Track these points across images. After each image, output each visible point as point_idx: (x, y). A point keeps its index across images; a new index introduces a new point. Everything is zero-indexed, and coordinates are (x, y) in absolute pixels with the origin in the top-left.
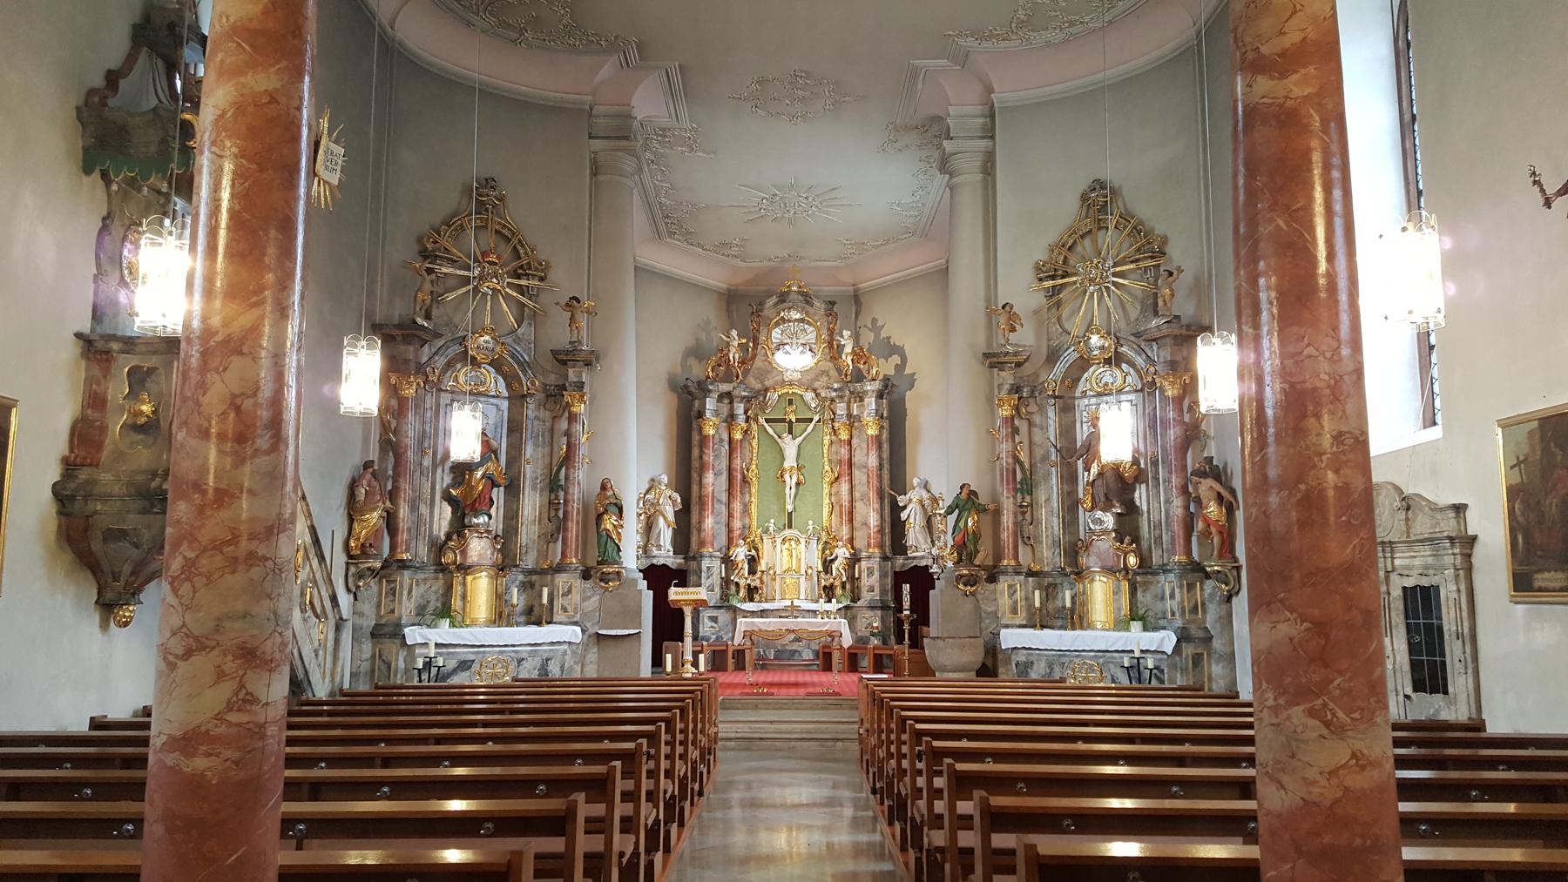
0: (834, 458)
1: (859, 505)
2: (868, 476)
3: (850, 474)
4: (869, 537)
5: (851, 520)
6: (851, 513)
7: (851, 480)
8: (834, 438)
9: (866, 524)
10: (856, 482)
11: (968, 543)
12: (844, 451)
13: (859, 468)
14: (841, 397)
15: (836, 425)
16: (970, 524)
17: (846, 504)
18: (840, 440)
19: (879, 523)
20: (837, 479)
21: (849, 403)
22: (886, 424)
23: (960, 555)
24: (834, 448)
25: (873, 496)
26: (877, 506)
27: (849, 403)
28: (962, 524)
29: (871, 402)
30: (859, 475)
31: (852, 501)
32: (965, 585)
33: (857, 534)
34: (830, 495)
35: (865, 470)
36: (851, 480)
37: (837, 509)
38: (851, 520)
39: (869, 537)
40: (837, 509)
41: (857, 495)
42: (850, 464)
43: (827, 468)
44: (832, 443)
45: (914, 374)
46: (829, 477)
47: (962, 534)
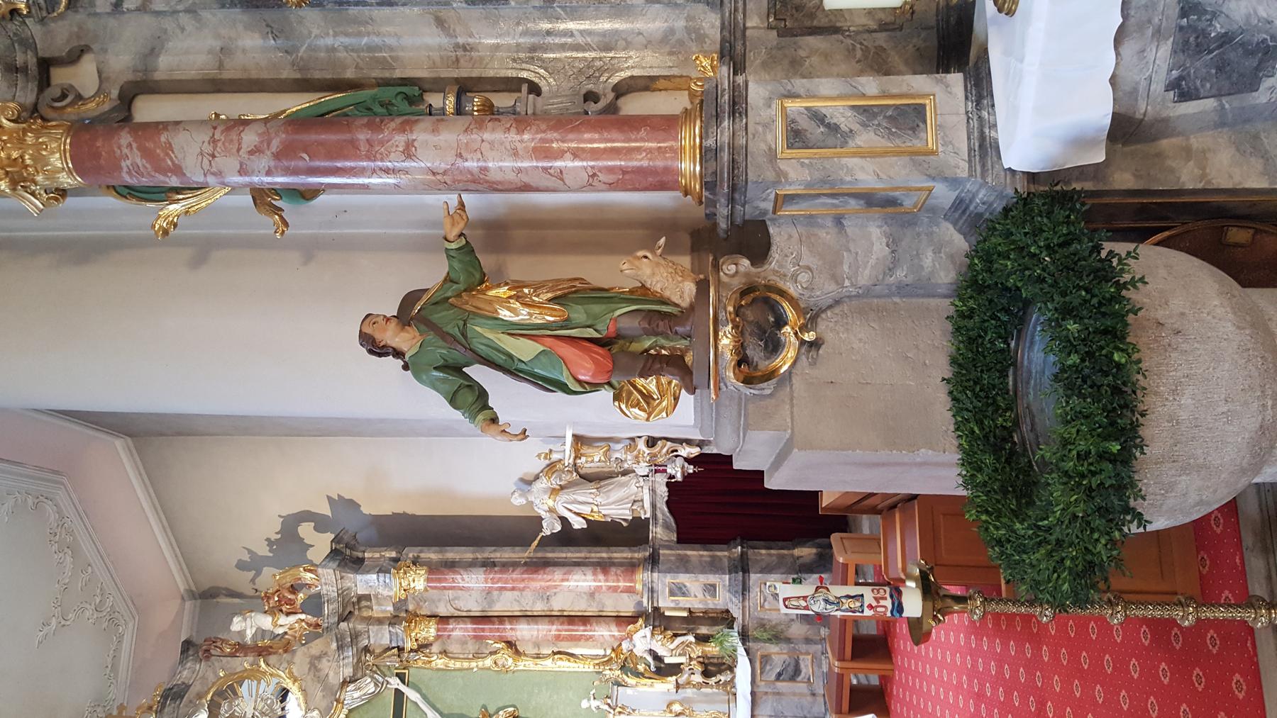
0: (472, 647)
1: (560, 604)
2: (501, 589)
3: (501, 619)
4: (615, 589)
5: (584, 620)
6: (571, 619)
7: (513, 618)
8: (435, 649)
9: (592, 595)
10: (515, 609)
11: (603, 329)
12: (459, 631)
13: (491, 603)
14: (355, 636)
15: (409, 645)
16: (523, 315)
17: (554, 629)
18: (438, 637)
19: (589, 571)
20: (510, 644)
21: (369, 620)
22: (411, 553)
23: (652, 364)
24: (454, 648)
25: (540, 581)
26: (558, 574)
27: (369, 620)
28: (524, 350)
29: (364, 583)
30: (505, 603)
31: (549, 617)
32: (774, 347)
33: (610, 609)
34: (538, 656)
35: (496, 593)
36: (513, 618)
37: (564, 646)
38: (584, 620)
39: (615, 589)
40: (564, 646)
41: (539, 607)
42: (484, 619)
43: (488, 662)
44: (444, 653)
45: (329, 498)
46: (506, 659)
47: (566, 350)
